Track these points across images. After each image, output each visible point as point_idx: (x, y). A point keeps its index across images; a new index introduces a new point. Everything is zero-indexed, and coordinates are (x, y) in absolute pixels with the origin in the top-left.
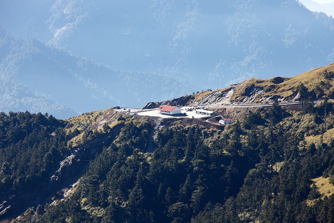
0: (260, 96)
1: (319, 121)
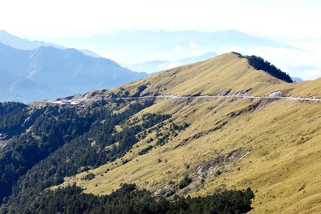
0: (97, 96)
1: (118, 105)
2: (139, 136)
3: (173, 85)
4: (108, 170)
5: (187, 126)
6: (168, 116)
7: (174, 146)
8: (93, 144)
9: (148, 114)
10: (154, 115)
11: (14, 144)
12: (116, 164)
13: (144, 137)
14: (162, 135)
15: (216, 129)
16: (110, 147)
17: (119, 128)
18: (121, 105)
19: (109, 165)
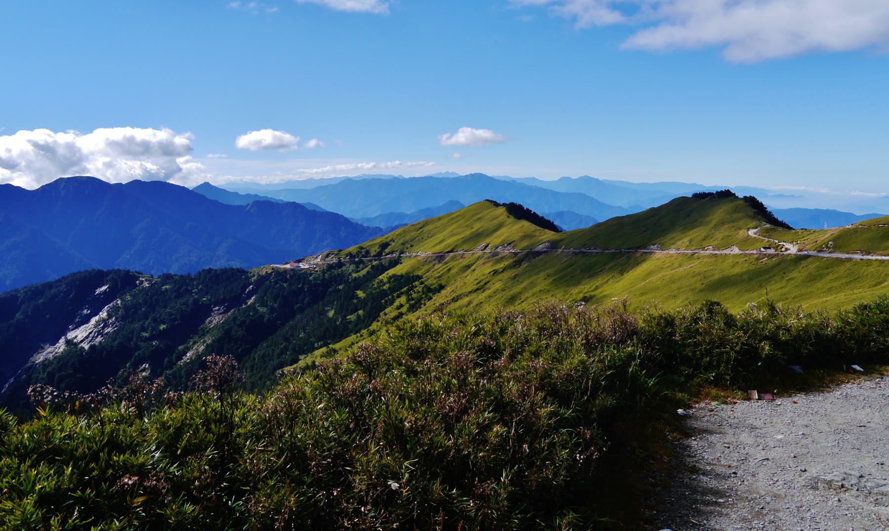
1: (357, 267)
2: (386, 302)
3: (422, 240)
4: (353, 344)
6: (419, 278)
7: (429, 312)
8: (331, 314)
9: (394, 276)
10: (402, 276)
11: (235, 319)
12: (361, 336)
13: (392, 302)
14: (413, 299)
15: (477, 289)
16: (352, 317)
17: (360, 294)
18: (361, 266)
19: (353, 338)
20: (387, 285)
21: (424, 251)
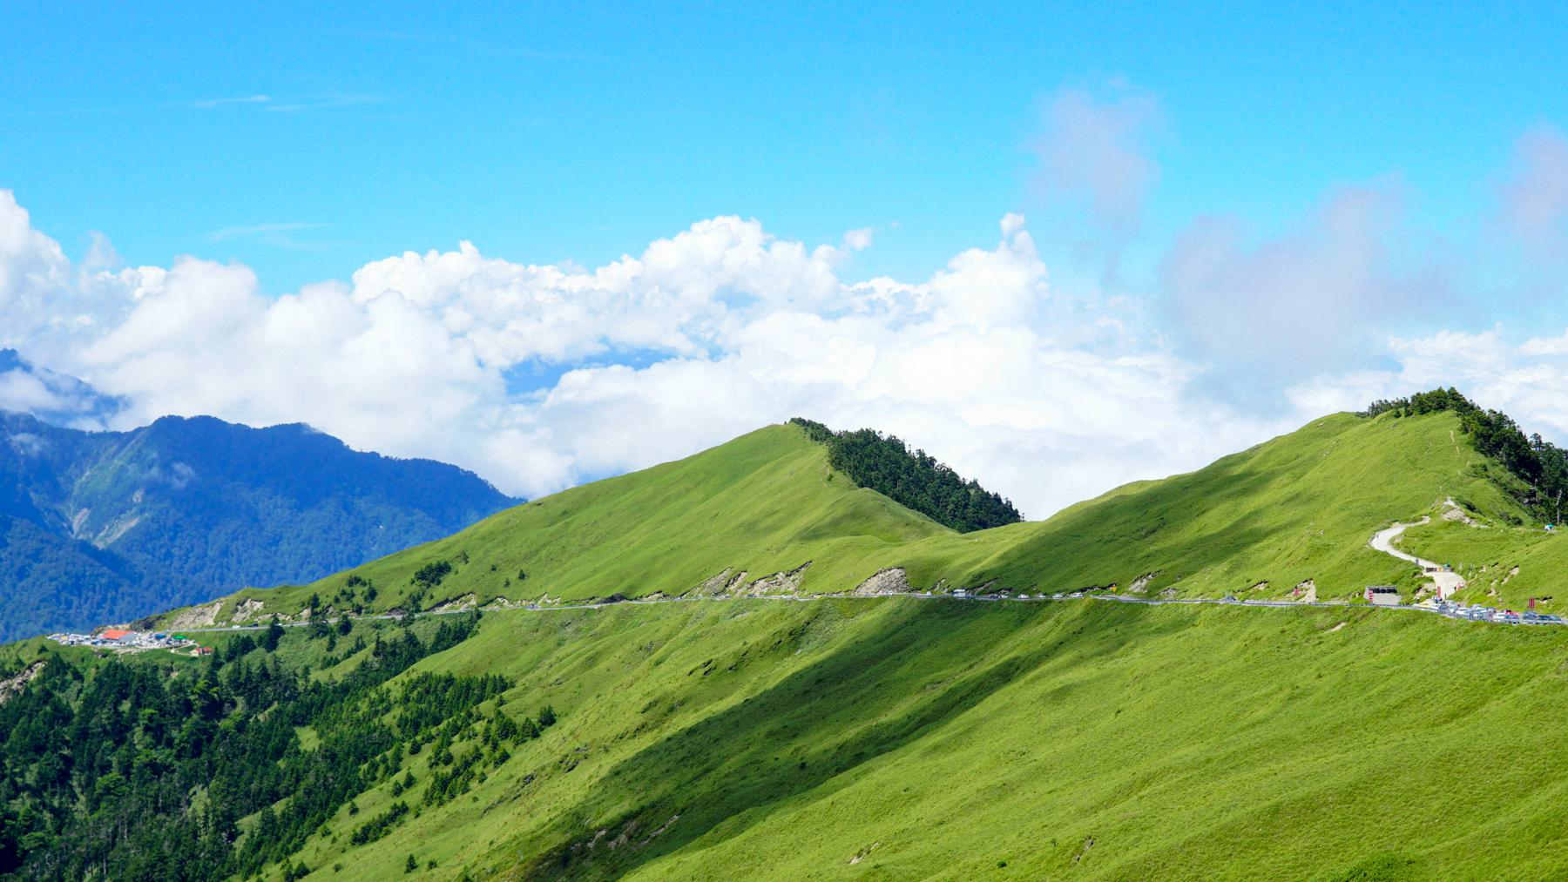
5: (549, 719)
9: (427, 677)
10: (450, 681)
14: (449, 760)
20: (397, 711)
21: (548, 597)
